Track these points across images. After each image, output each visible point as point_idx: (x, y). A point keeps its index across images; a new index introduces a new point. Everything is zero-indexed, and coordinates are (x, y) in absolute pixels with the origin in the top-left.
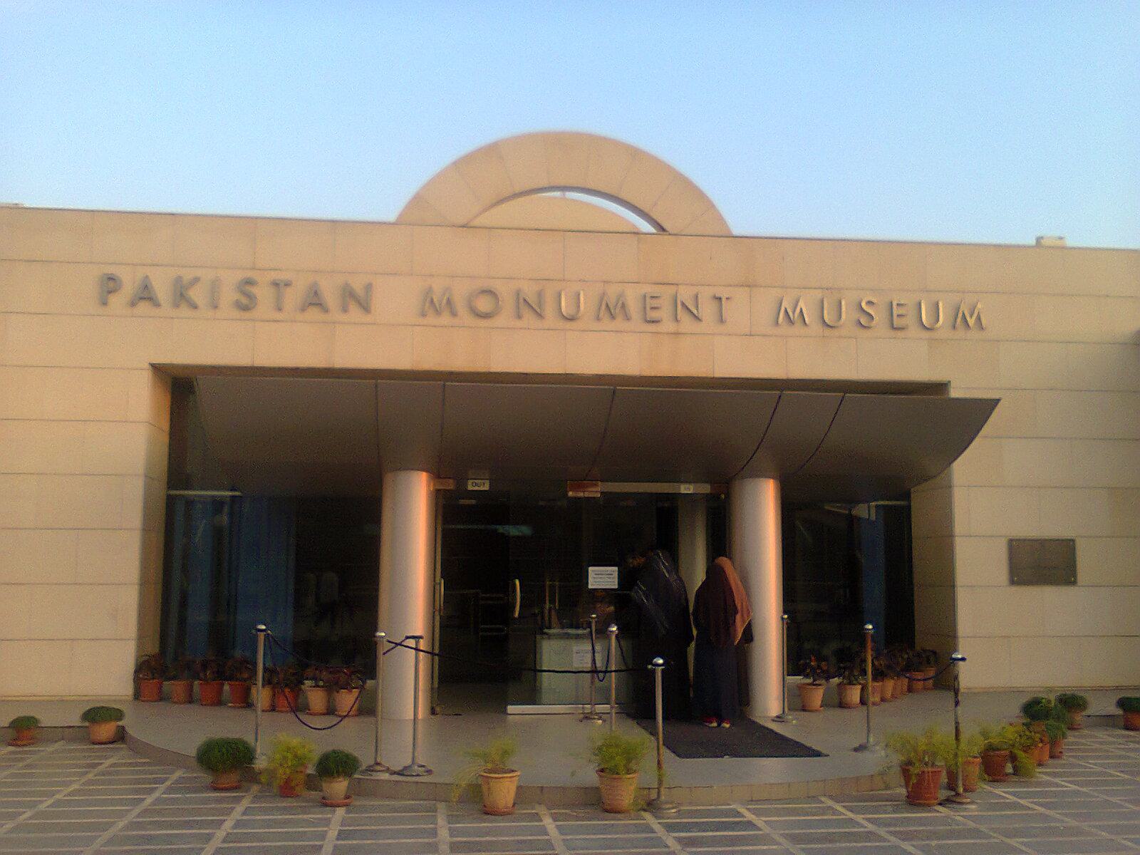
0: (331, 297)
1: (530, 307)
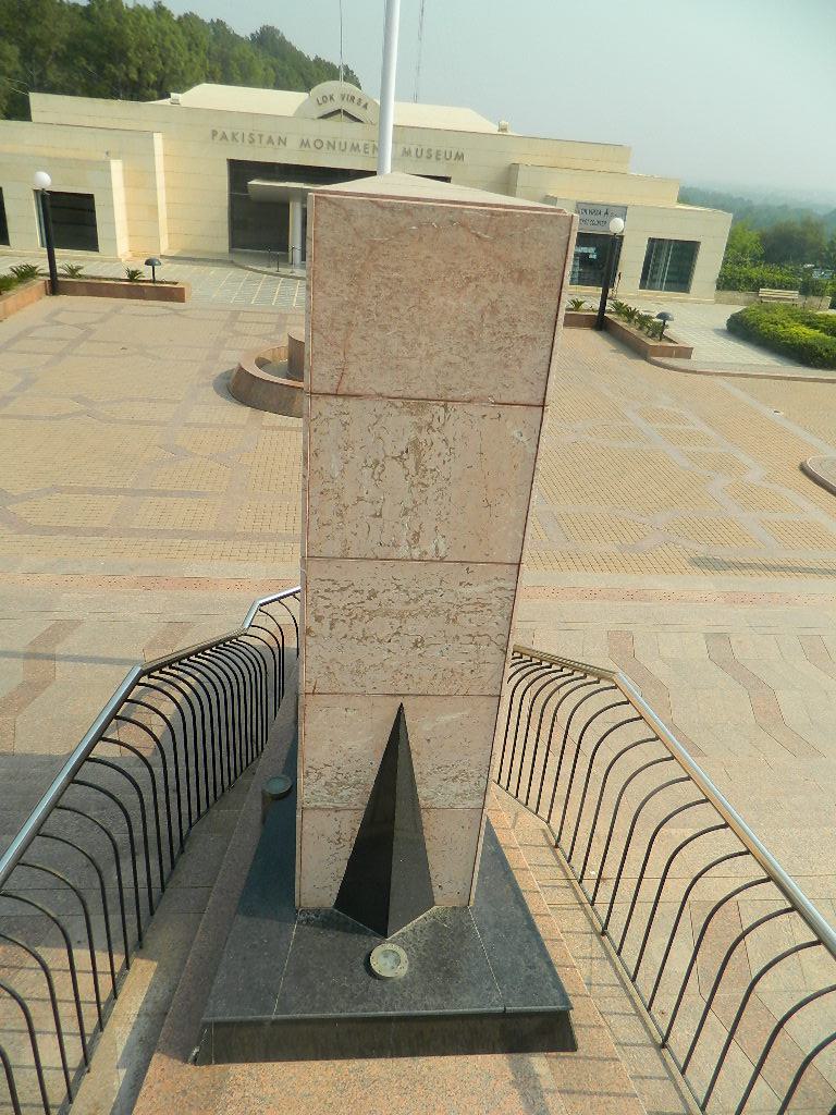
0: (275, 139)
1: (331, 146)
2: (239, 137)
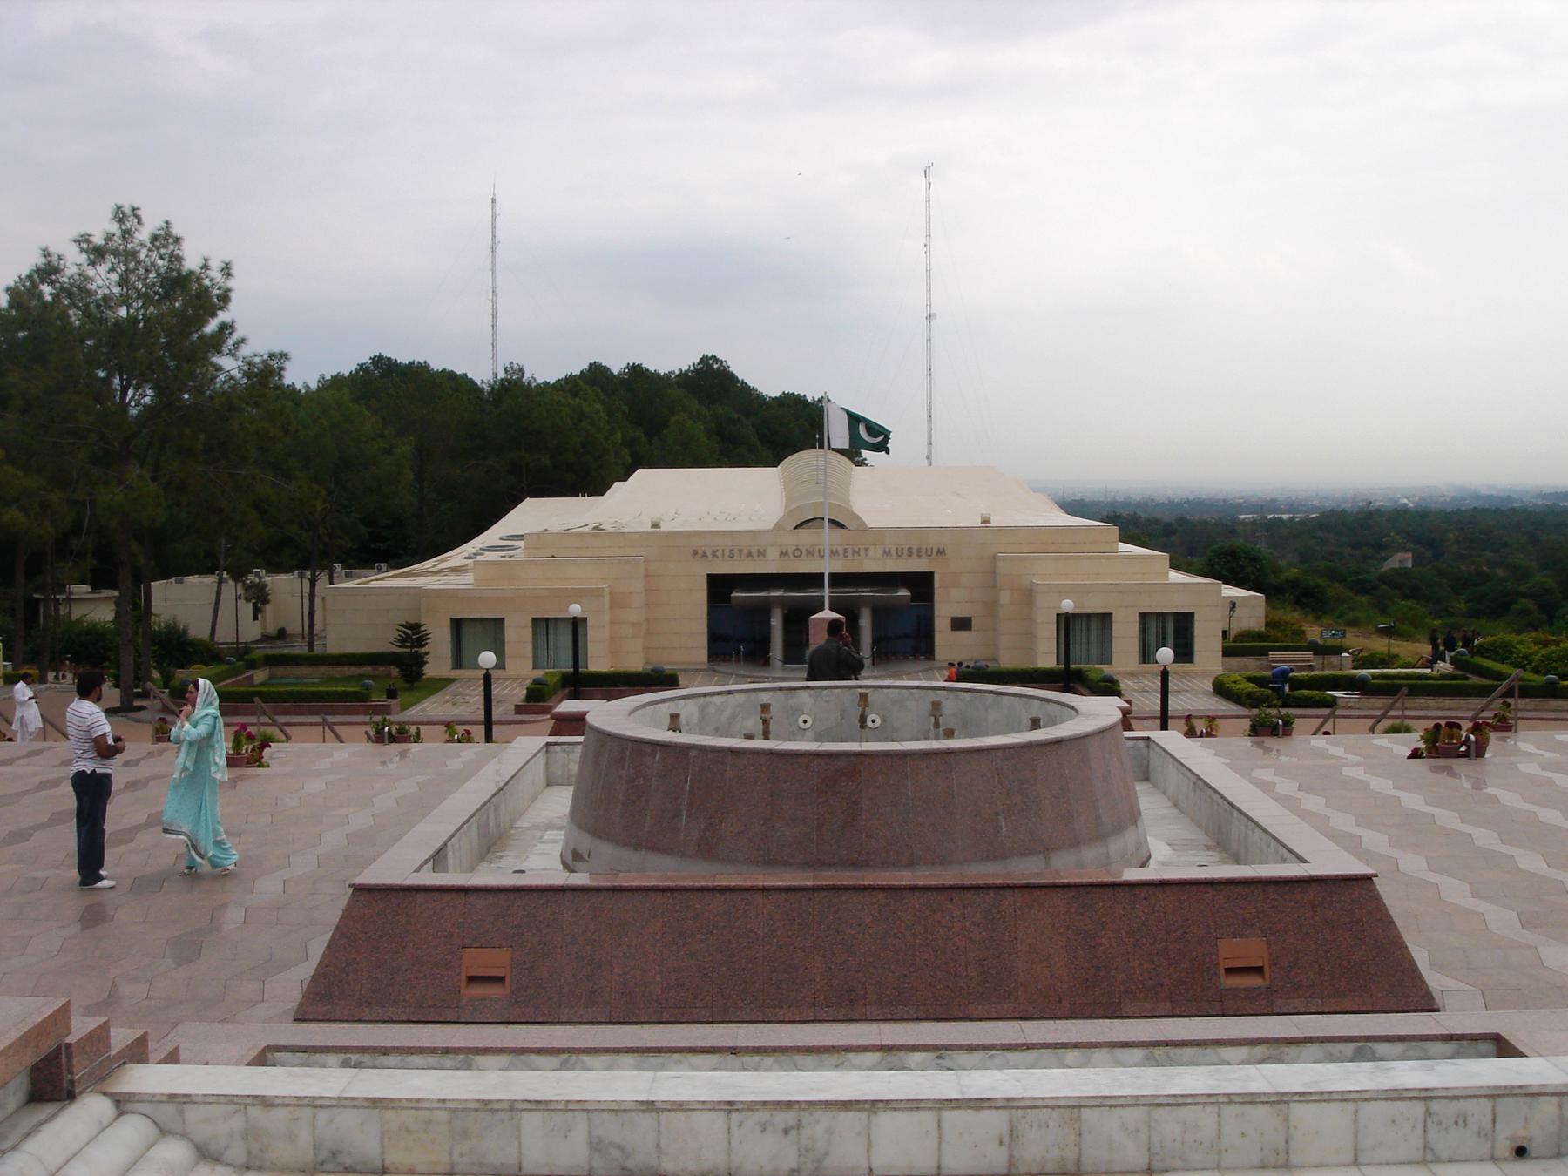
0: (754, 552)
1: (810, 553)
2: (719, 554)
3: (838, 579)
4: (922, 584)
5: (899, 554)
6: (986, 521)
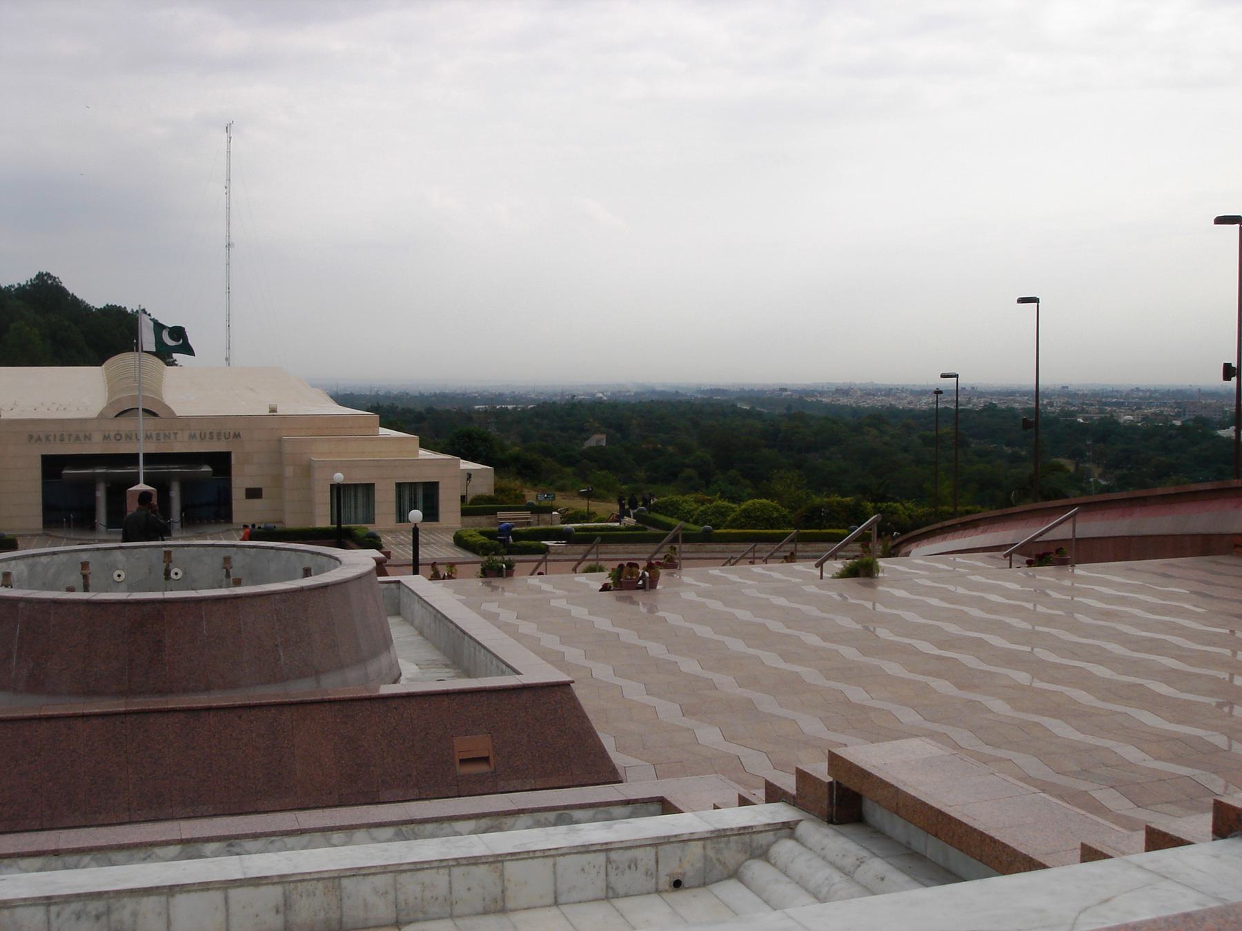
0: (81, 436)
1: (129, 437)
3: (151, 458)
4: (221, 462)
5: (202, 438)
6: (273, 410)
